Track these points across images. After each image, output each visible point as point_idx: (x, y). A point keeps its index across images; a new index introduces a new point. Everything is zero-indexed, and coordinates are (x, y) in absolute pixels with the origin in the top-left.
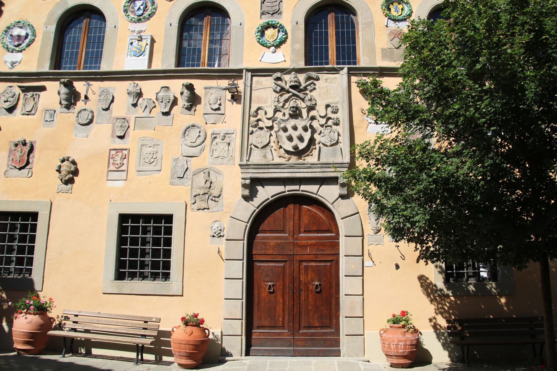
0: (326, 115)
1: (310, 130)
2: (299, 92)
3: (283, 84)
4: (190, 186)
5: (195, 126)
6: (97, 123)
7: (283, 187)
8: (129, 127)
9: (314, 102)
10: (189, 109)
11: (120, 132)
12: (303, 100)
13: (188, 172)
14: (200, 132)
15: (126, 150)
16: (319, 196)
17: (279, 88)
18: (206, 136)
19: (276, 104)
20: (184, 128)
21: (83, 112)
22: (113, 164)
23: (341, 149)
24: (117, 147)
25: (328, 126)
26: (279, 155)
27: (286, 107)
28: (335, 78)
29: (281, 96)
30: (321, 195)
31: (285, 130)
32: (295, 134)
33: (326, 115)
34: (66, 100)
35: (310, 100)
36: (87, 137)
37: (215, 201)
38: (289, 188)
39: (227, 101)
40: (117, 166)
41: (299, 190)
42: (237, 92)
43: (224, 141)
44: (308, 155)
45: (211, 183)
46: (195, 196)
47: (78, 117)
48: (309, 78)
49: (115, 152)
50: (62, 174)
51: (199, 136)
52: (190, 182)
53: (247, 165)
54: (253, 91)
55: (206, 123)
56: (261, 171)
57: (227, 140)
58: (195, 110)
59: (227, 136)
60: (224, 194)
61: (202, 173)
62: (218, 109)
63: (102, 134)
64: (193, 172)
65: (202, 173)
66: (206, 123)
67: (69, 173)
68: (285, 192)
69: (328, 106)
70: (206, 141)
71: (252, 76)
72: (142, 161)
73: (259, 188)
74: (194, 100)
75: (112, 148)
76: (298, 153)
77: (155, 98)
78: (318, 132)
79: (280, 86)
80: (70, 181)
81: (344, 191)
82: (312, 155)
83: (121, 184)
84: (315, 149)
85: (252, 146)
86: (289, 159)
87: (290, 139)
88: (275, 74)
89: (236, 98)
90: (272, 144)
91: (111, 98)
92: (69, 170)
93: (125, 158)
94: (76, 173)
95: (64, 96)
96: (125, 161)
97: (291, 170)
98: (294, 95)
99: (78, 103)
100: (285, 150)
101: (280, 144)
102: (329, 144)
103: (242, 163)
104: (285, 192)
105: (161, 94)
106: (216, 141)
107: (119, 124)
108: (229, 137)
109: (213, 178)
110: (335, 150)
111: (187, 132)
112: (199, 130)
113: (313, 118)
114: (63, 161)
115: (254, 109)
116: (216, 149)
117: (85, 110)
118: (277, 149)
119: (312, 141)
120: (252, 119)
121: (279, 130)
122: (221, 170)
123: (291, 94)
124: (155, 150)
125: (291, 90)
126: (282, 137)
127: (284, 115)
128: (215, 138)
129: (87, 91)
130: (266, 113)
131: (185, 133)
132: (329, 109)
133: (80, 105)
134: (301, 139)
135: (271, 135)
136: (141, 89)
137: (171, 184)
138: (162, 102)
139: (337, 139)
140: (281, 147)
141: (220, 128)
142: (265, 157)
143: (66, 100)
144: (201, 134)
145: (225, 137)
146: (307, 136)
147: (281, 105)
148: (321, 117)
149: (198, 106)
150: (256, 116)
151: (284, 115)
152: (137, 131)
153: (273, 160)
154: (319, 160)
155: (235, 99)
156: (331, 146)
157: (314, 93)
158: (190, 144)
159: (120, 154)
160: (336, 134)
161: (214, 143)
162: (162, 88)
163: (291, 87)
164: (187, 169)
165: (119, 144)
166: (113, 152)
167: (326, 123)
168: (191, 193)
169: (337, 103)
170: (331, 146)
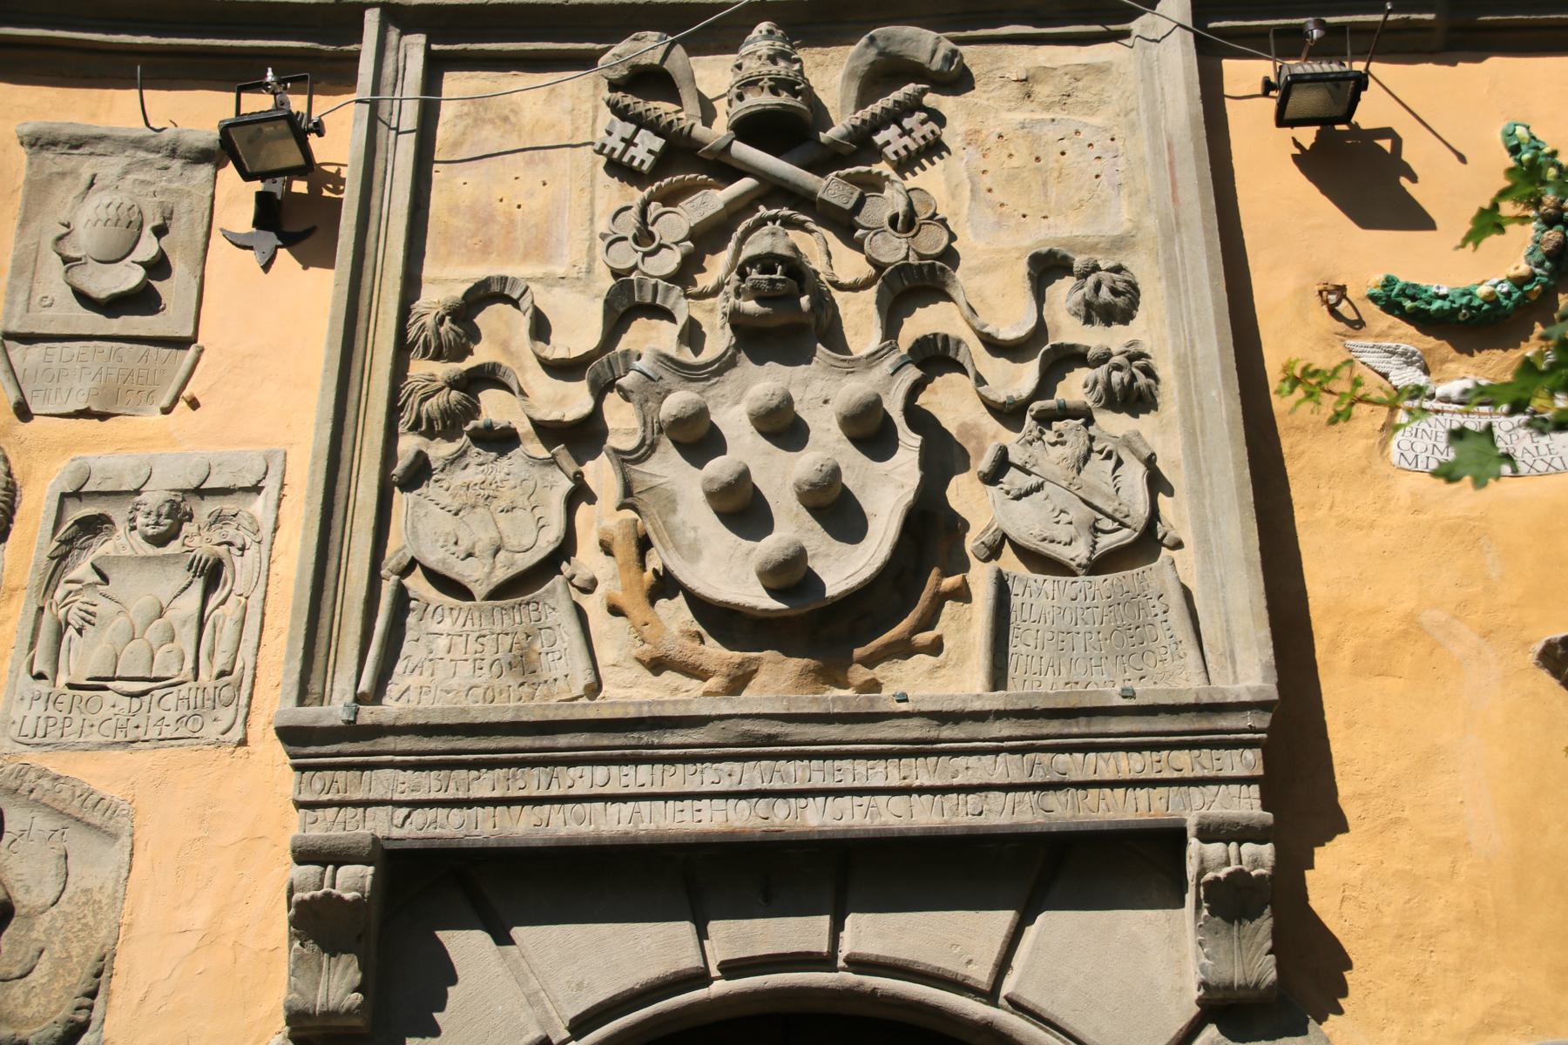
0: (1040, 331)
1: (910, 443)
2: (820, 168)
3: (686, 116)
7: (686, 929)
9: (931, 241)
12: (844, 224)
16: (1017, 1006)
17: (647, 145)
19: (626, 256)
23: (1187, 594)
25: (1065, 412)
26: (647, 651)
27: (705, 281)
28: (1100, 70)
29: (670, 198)
30: (1031, 997)
31: (699, 440)
32: (780, 475)
33: (1040, 331)
35: (907, 222)
38: (734, 937)
39: (217, 241)
41: (825, 962)
42: (308, 168)
43: (174, 547)
44: (904, 649)
48: (883, 74)
53: (352, 731)
54: (439, 174)
55: (23, 412)
56: (485, 784)
57: (199, 540)
59: (204, 509)
62: (142, 300)
66: (23, 412)
68: (700, 978)
69: (1047, 268)
71: (435, 67)
73: (466, 947)
76: (818, 627)
78: (984, 463)
79: (655, 127)
81: (1253, 961)
82: (936, 648)
84: (962, 594)
85: (416, 583)
86: (738, 682)
87: (743, 509)
88: (618, 48)
89: (295, 221)
90: (587, 561)
97: (753, 775)
98: (774, 191)
100: (702, 607)
101: (654, 561)
102: (1079, 552)
103: (309, 715)
104: (700, 978)
106: (103, 548)
108: (219, 519)
110: (1133, 601)
113: (935, 357)
115: (444, 284)
116: (89, 618)
118: (634, 602)
119: (931, 531)
120: (420, 368)
121: (646, 450)
122: (114, 793)
123: (746, 183)
125: (742, 150)
126: (670, 503)
127: (692, 335)
128: (93, 526)
130: (540, 328)
132: (1063, 292)
134: (837, 510)
135: (580, 494)
139: (1141, 510)
140: (665, 585)
141: (150, 449)
142: (523, 665)
146: (888, 490)
147: (669, 261)
148: (995, 346)
150: (461, 353)
151: (692, 335)
153: (594, 689)
154: (998, 678)
155: (291, 227)
156: (1101, 564)
157: (931, 179)
160: (1134, 474)
161: (82, 569)
163: (748, 128)
167: (1045, 387)
169: (1120, 243)
170: (1101, 564)
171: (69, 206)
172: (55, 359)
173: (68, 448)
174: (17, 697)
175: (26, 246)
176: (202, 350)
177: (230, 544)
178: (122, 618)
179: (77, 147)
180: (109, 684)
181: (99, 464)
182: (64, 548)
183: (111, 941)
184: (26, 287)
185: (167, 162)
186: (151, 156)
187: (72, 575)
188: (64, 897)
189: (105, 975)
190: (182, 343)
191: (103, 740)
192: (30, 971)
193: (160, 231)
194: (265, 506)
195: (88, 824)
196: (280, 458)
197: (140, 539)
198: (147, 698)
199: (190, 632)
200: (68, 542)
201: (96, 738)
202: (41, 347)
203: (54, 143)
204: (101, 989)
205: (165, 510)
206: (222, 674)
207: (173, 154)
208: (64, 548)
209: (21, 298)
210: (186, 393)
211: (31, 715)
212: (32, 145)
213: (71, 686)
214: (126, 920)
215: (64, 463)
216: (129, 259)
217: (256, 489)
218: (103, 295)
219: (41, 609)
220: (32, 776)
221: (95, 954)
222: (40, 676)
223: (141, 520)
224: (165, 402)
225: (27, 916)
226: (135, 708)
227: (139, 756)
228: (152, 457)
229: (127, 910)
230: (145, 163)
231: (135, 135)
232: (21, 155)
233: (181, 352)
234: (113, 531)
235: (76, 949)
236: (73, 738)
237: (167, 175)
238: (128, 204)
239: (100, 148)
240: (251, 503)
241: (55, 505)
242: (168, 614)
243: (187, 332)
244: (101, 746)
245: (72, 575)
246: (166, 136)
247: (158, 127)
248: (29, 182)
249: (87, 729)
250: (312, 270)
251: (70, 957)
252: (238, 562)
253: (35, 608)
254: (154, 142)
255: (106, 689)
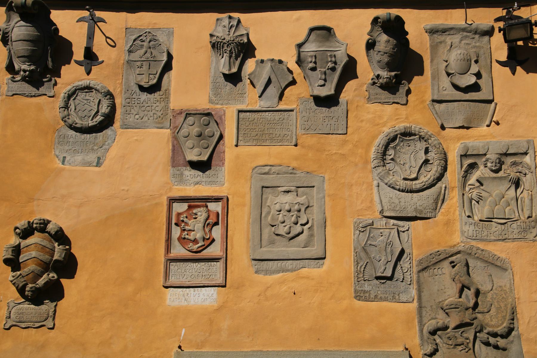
4: (415, 304)
5: (410, 134)
6: (125, 126)
8: (221, 137)
10: (390, 88)
11: (196, 150)
13: (404, 263)
14: (427, 151)
15: (217, 199)
18: (446, 161)
20: (380, 140)
21: (81, 96)
22: (182, 240)
24: (191, 191)
34: (29, 58)
36: (98, 164)
37: (496, 347)
40: (195, 247)
43: (501, 174)
45: (478, 293)
46: (433, 333)
47: (66, 107)
49: (184, 207)
50: (25, 271)
51: (426, 162)
52: (414, 292)
57: (508, 171)
58: (409, 92)
59: (509, 160)
60: (522, 326)
61: (446, 264)
62: (475, 88)
63: (139, 160)
64: (420, 262)
65: (446, 264)
66: (443, 128)
67: (46, 267)
70: (448, 174)
72: (267, 231)
74: (403, 66)
75: (177, 193)
77: (295, 58)
80: (54, 293)
83: (207, 297)
91: (165, 58)
92: (45, 257)
93: (217, 224)
94: (68, 267)
95: (21, 48)
96: (217, 232)
99: (65, 70)
105: (311, 48)
107: (191, 128)
108: (514, 164)
109: (480, 277)
111: (391, 152)
112: (423, 145)
114: (26, 233)
117: (88, 88)
122: (503, 256)
124: (302, 199)
128: (473, 166)
129: (91, 37)
131: (384, 154)
133: (71, 75)
136: (248, 35)
137: (358, 297)
138: (314, 69)
143: (29, 58)
144: (432, 155)
145: (501, 163)
149: (416, 79)
152: (245, 150)
158: (403, 184)
159: (201, 213)
161: (472, 180)
162: (312, 30)
164: (402, 252)
165: (195, 185)
166: (180, 208)
168: (421, 325)
171: (445, 54)
172: (449, 109)
173: (459, 139)
174: (464, 224)
175: (434, 69)
176: (496, 104)
177: (520, 172)
178: (490, 199)
179: (444, 32)
180: (493, 220)
181: (470, 145)
182: (466, 174)
183: (514, 303)
184: (437, 84)
185: (473, 36)
186: (468, 34)
187: (470, 183)
188: (494, 288)
189: (515, 313)
190: (490, 102)
191: (495, 238)
192: (490, 311)
193: (476, 62)
194: (531, 160)
195: (496, 265)
196: (532, 143)
197: (489, 170)
198: (506, 225)
199: (513, 203)
200: (466, 172)
201: (493, 238)
202: (444, 105)
203: (437, 31)
204: (515, 318)
205: (498, 161)
206: (529, 217)
207: (476, 33)
208: (466, 174)
209: (436, 88)
210: (494, 119)
211: (470, 230)
212: (430, 33)
213: (480, 220)
214: (517, 296)
215: (459, 144)
216: (469, 73)
217: (526, 154)
218: (464, 86)
219: (463, 194)
220: (474, 249)
221: (509, 306)
222: (469, 217)
223: (489, 165)
224: (487, 123)
225: (484, 293)
226: (503, 228)
227: (508, 244)
228: (488, 142)
229: (516, 293)
230: (466, 37)
231: (463, 27)
232: (427, 36)
233: (488, 105)
234: (478, 168)
235: (502, 305)
236: (485, 237)
237: (474, 40)
238: (466, 52)
239: (452, 32)
240: (524, 158)
241: (460, 159)
242: (505, 196)
243: (491, 98)
244: (495, 240)
245: (470, 183)
246: (474, 26)
247: (470, 23)
248: (431, 46)
249: (489, 235)
250: (530, 74)
251: (501, 307)
252: (524, 179)
253: (461, 194)
254: (469, 29)
255: (492, 221)
